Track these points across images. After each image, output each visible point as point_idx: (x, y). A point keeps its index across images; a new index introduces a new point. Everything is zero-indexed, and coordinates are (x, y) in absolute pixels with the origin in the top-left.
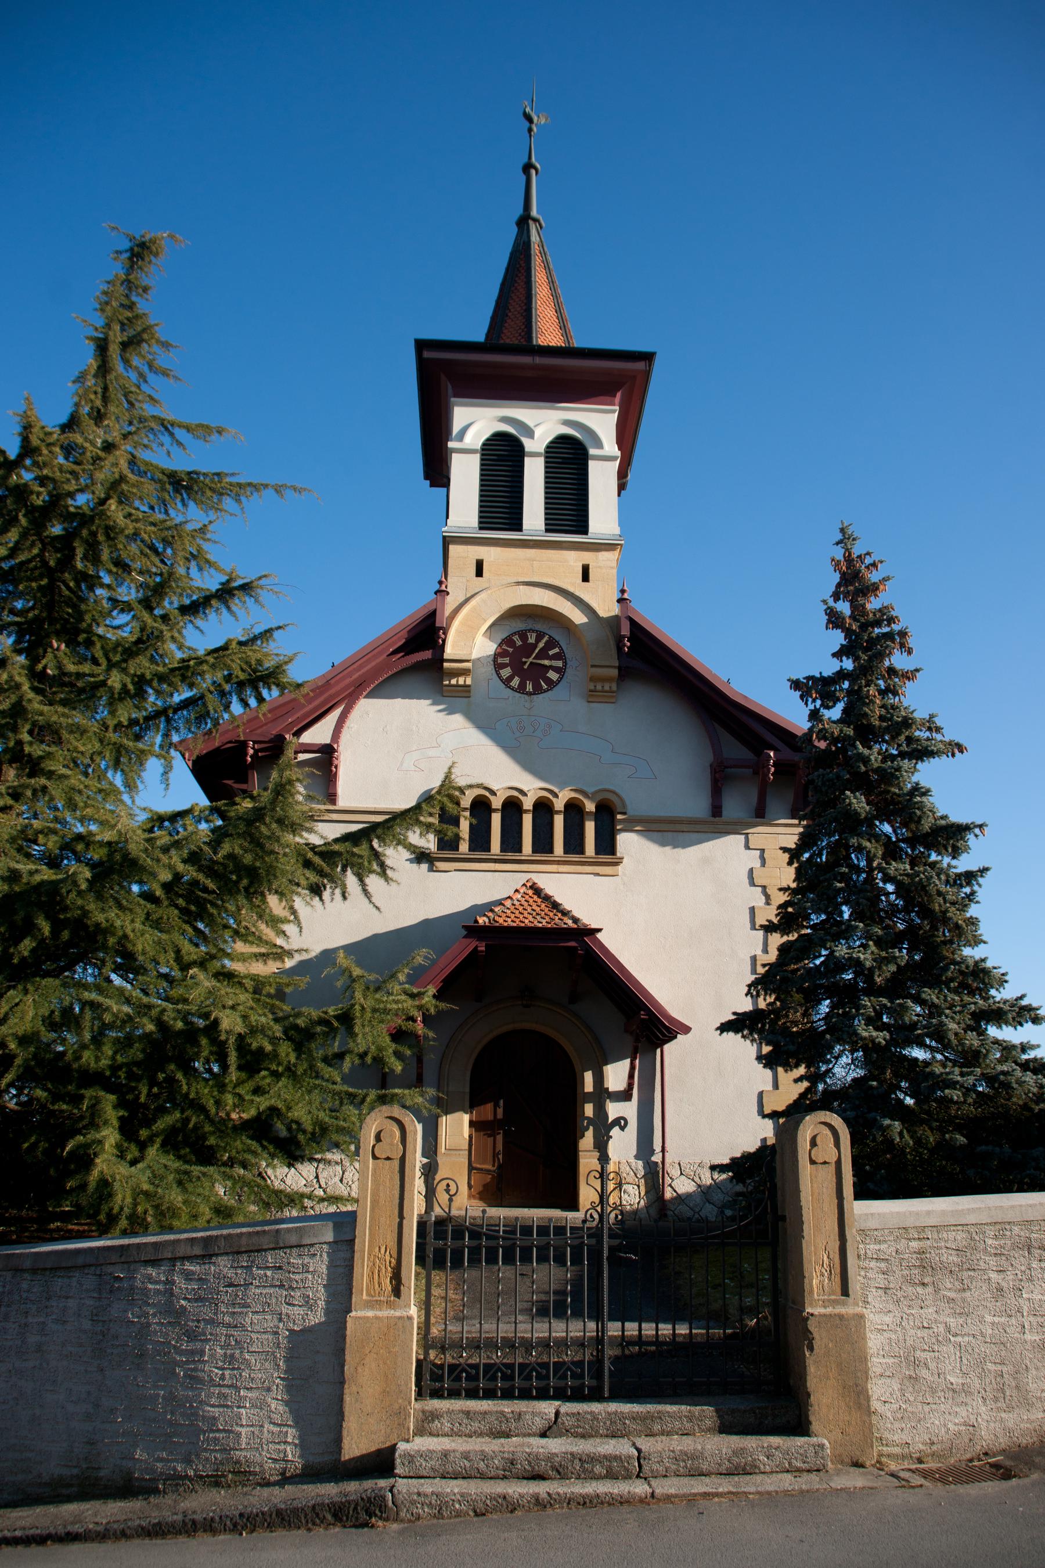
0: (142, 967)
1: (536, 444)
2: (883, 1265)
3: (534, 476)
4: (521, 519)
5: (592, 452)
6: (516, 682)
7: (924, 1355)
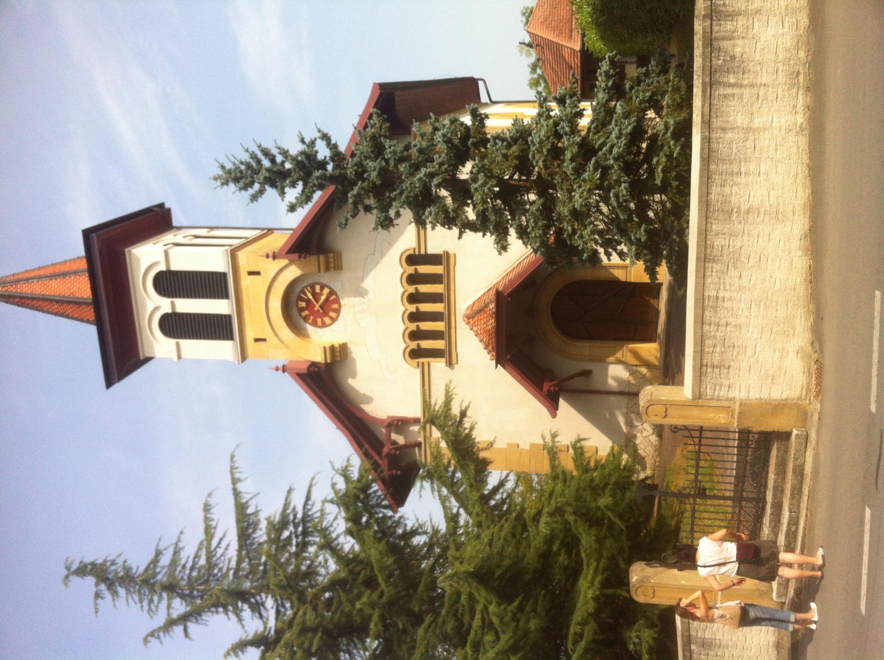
0: (446, 142)
1: (165, 305)
2: (717, 387)
3: (188, 306)
4: (221, 316)
5: (162, 267)
6: (332, 314)
7: (763, 371)
